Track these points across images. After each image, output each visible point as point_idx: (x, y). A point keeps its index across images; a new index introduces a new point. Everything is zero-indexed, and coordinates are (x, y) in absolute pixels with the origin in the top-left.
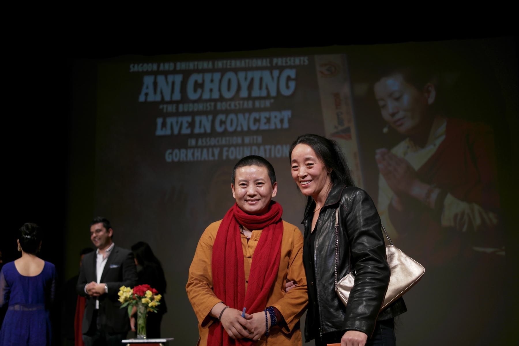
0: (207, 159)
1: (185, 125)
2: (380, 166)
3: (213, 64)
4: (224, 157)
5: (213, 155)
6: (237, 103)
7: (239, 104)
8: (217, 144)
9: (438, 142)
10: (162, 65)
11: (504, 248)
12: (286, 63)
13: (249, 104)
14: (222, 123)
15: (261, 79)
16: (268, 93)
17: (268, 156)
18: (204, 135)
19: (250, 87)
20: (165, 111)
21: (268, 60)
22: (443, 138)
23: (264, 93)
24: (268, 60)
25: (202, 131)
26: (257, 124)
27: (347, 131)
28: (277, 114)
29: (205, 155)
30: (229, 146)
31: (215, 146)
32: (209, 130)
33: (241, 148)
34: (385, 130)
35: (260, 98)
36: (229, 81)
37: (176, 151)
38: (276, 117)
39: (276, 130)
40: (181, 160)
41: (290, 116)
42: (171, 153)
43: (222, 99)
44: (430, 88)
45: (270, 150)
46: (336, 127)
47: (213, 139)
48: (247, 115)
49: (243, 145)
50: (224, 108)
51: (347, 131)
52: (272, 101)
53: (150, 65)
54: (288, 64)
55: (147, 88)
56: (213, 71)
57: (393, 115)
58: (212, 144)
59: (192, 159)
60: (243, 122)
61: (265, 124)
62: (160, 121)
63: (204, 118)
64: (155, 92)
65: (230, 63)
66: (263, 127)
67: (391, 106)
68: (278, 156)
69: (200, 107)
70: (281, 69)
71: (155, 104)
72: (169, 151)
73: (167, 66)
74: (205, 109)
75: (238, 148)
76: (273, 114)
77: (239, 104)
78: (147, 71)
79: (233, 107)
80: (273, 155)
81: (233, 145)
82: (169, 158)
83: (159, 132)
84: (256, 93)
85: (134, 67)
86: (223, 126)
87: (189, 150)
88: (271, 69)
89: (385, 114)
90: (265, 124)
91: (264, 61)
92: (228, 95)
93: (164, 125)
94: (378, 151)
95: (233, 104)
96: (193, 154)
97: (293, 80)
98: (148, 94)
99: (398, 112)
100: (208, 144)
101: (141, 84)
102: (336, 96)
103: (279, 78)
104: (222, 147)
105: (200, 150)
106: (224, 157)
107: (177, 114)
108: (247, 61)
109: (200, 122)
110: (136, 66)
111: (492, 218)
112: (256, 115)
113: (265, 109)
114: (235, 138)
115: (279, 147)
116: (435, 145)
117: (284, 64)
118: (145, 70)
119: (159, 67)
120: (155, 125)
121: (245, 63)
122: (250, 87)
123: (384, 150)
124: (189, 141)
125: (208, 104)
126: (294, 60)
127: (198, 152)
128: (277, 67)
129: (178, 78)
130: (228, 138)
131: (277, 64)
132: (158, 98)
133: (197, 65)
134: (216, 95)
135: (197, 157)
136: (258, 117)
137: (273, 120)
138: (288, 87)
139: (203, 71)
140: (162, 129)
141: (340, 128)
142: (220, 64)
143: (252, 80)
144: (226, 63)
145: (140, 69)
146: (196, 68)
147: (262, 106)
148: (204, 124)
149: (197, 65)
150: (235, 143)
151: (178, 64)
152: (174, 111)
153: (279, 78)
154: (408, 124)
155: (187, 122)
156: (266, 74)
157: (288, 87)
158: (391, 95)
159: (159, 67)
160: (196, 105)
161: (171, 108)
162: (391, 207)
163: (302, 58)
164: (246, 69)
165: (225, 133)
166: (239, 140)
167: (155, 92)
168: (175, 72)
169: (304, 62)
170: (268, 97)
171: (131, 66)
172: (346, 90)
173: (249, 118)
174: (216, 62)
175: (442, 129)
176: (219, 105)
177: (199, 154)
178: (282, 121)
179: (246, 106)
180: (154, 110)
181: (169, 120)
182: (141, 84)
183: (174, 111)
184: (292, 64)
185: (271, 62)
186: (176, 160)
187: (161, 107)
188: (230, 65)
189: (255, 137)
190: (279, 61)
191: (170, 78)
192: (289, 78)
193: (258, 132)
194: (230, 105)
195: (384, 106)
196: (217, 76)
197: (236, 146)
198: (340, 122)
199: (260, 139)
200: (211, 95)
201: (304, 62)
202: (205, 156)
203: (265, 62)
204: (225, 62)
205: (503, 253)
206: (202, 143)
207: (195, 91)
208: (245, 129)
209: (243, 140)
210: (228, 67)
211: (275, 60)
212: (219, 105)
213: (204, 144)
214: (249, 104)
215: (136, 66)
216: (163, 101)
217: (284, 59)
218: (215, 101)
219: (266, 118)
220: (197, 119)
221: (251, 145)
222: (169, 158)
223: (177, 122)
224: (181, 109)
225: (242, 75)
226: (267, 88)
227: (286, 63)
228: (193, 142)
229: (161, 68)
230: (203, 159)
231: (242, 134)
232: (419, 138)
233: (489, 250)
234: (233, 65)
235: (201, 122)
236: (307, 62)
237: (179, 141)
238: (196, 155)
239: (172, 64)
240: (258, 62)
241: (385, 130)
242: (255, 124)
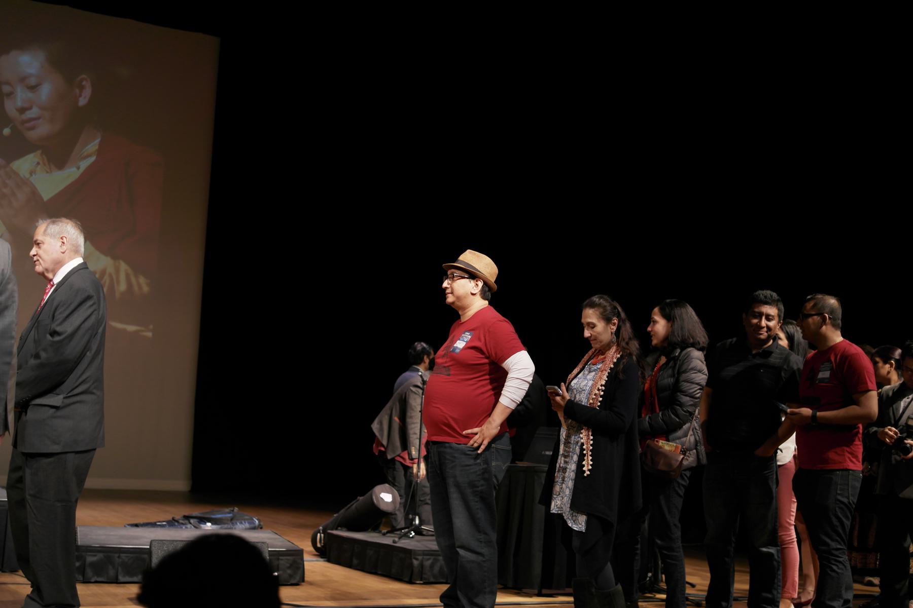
9: (84, 165)
11: (151, 327)
22: (93, 159)
34: (6, 131)
44: (84, 83)
57: (22, 110)
67: (21, 96)
89: (10, 107)
99: (30, 108)
111: (143, 284)
116: (78, 168)
154: (43, 130)
158: (23, 79)
175: (93, 146)
195: (10, 94)
205: (150, 334)
232: (57, 154)
233: (131, 328)
241: (6, 131)
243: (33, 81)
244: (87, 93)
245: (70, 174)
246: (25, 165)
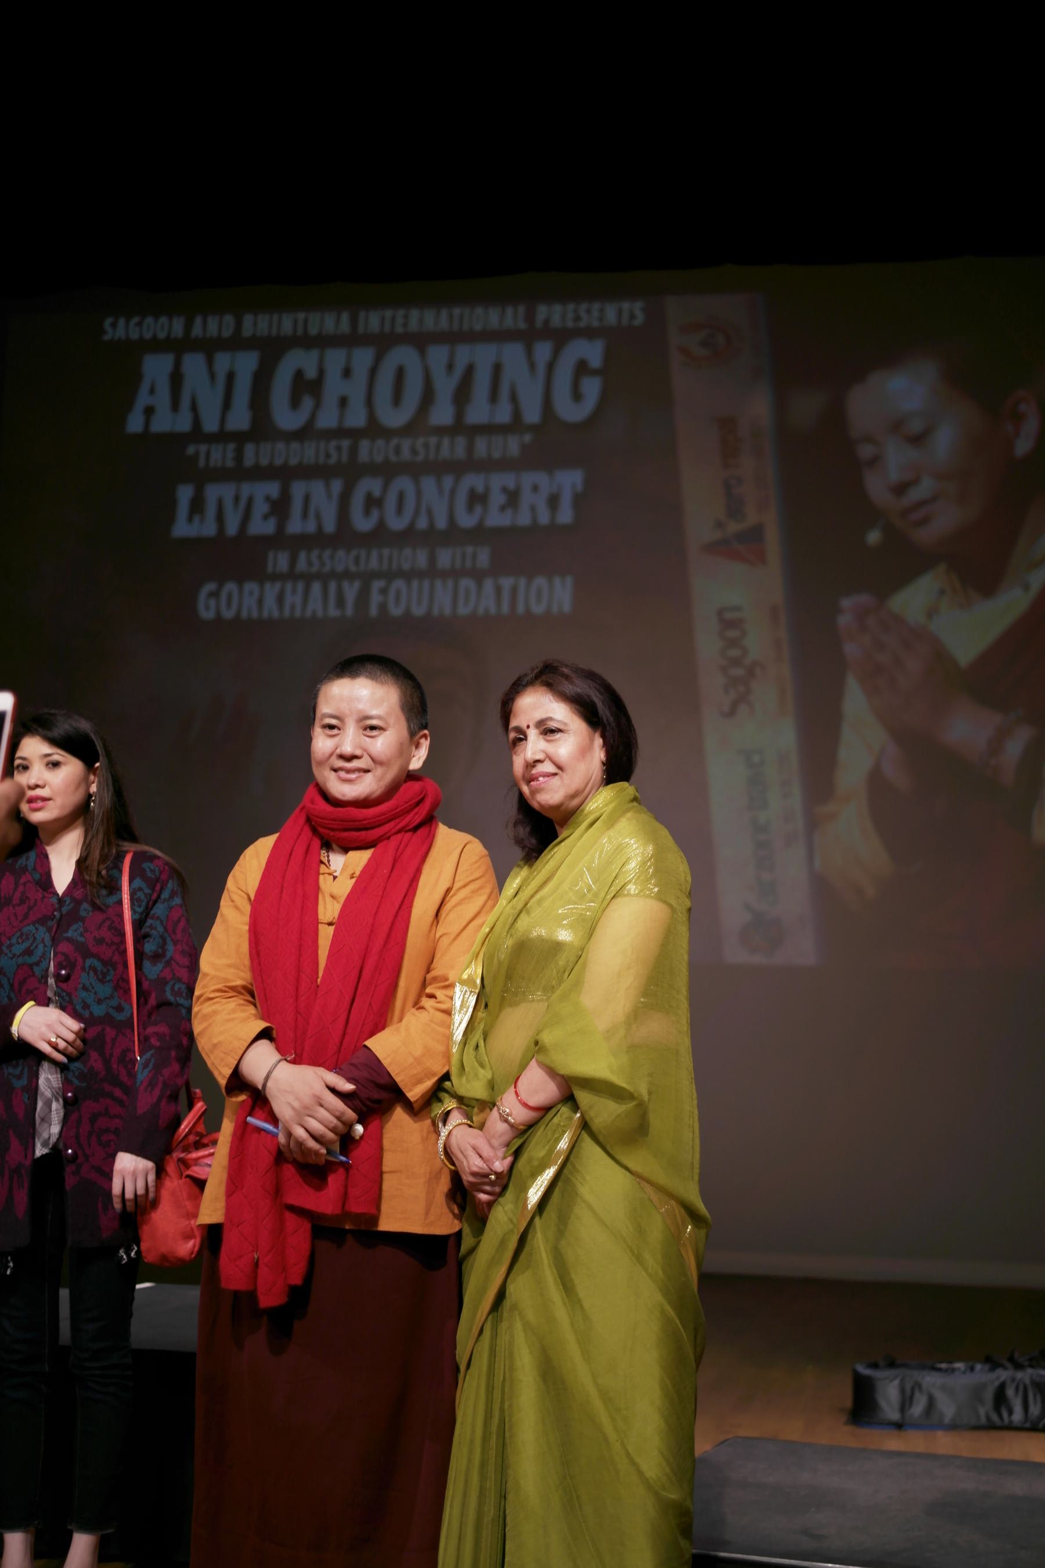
0: (320, 614)
1: (261, 508)
2: (851, 649)
3: (354, 321)
4: (374, 611)
5: (341, 603)
6: (420, 441)
7: (426, 446)
8: (353, 568)
10: (198, 321)
12: (578, 318)
13: (455, 448)
14: (372, 503)
15: (497, 369)
16: (517, 413)
17: (505, 609)
18: (318, 540)
19: (462, 395)
20: (202, 463)
21: (521, 309)
23: (503, 414)
24: (521, 309)
25: (311, 527)
26: (478, 509)
27: (754, 535)
28: (541, 478)
29: (315, 603)
30: (390, 576)
31: (347, 575)
32: (330, 526)
33: (426, 583)
34: (874, 537)
35: (489, 429)
36: (400, 374)
37: (231, 587)
38: (535, 488)
39: (534, 528)
40: (244, 615)
41: (579, 488)
42: (215, 594)
43: (374, 429)
44: (1023, 407)
45: (514, 590)
46: (720, 525)
47: (341, 553)
48: (448, 481)
49: (432, 572)
50: (379, 459)
51: (754, 535)
52: (528, 438)
53: (163, 320)
54: (582, 324)
55: (152, 391)
56: (352, 340)
57: (900, 489)
58: (340, 568)
59: (276, 614)
60: (435, 501)
61: (503, 508)
62: (185, 494)
63: (317, 488)
64: (175, 406)
65: (406, 317)
66: (496, 519)
67: (897, 459)
68: (538, 609)
69: (309, 452)
70: (561, 337)
71: (175, 441)
72: (210, 587)
73: (215, 326)
74: (321, 460)
75: (415, 583)
76: (528, 479)
77: (426, 446)
78: (154, 338)
79: (406, 454)
80: (521, 609)
81: (401, 574)
82: (207, 608)
83: (182, 528)
84: (478, 412)
85: (114, 325)
86: (375, 514)
87: (268, 586)
88: (528, 337)
89: (877, 487)
90: (503, 508)
91: (509, 311)
92: (393, 418)
93: (197, 506)
94: (846, 603)
95: (406, 444)
96: (280, 599)
97: (595, 372)
98: (155, 407)
99: (915, 482)
100: (327, 568)
101: (130, 380)
102: (727, 425)
103: (551, 366)
104: (367, 578)
105: (301, 586)
106: (374, 611)
107: (239, 473)
108: (457, 311)
109: (307, 499)
110: (122, 322)
112: (474, 481)
113: (504, 465)
114: (408, 551)
115: (540, 581)
116: (1026, 587)
117: (570, 324)
118: (148, 336)
119: (188, 326)
120: (172, 503)
121: (451, 317)
122: (462, 395)
123: (864, 599)
124: (271, 556)
125: (333, 444)
126: (602, 311)
127: (294, 592)
128: (548, 333)
129: (247, 363)
130: (386, 552)
131: (547, 322)
132: (183, 424)
133: (306, 321)
134: (356, 418)
135: (293, 607)
136: (480, 489)
137: (527, 498)
138: (577, 396)
139: (322, 342)
140: (190, 519)
141: (734, 527)
142: (373, 321)
143: (470, 371)
144: (393, 319)
145: (134, 335)
146: (300, 331)
147: (497, 455)
148: (318, 504)
149: (306, 321)
150: (406, 566)
151: (248, 319)
152: (230, 463)
153: (551, 366)
154: (945, 521)
155: (268, 498)
156: (513, 354)
157: (577, 396)
158: (897, 426)
159: (188, 326)
160: (295, 445)
161: (220, 456)
162: (876, 779)
163: (626, 306)
164: (453, 338)
165: (379, 536)
166: (421, 559)
167: (175, 406)
168: (236, 343)
169: (632, 317)
170: (516, 425)
171: (108, 321)
172: (758, 408)
173: (453, 492)
174: (362, 315)
176: (365, 450)
177: (298, 599)
178: (553, 501)
179: (445, 452)
180: (170, 460)
181: (213, 492)
182: (139, 377)
183: (230, 463)
184: (596, 324)
185: (530, 317)
186: (228, 614)
187: (191, 450)
188: (405, 325)
189: (469, 550)
190: (554, 314)
191: (223, 361)
192: (582, 368)
193: (479, 534)
194: (398, 450)
195: (875, 461)
196: (363, 358)
197: (409, 575)
198: (735, 508)
199: (483, 557)
200: (341, 417)
201: (632, 317)
202: (315, 606)
203: (511, 317)
204: (388, 313)
206: (310, 564)
207: (295, 403)
208: (441, 523)
209: (432, 560)
210: (399, 330)
211: (542, 312)
212: (364, 445)
213: (315, 569)
214: (455, 448)
215: (122, 322)
216: (197, 434)
217: (571, 307)
218: (354, 434)
219: (504, 490)
220: (298, 489)
221: (455, 574)
222: (207, 608)
223: (237, 499)
224: (249, 461)
225: (438, 355)
226: (514, 398)
227: (578, 318)
228: (280, 561)
229: (197, 331)
230: (308, 614)
231: (432, 538)
232: (978, 567)
234: (414, 325)
235: (307, 499)
236: (640, 319)
237: (238, 557)
238: (289, 599)
239: (229, 319)
240: (492, 317)
241: (874, 537)
242: (470, 508)
243: (916, 426)
244: (1031, 426)
245: (1010, 604)
246: (915, 599)
